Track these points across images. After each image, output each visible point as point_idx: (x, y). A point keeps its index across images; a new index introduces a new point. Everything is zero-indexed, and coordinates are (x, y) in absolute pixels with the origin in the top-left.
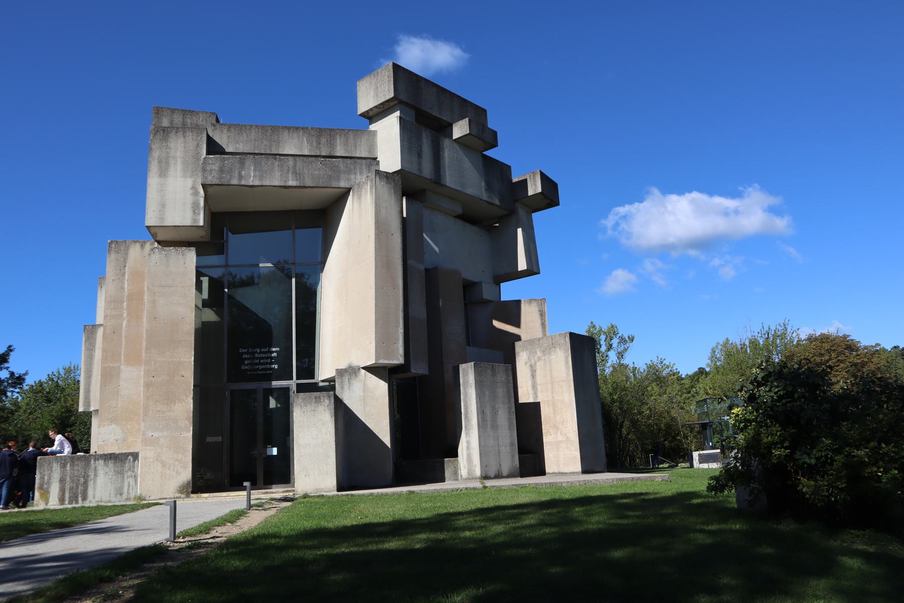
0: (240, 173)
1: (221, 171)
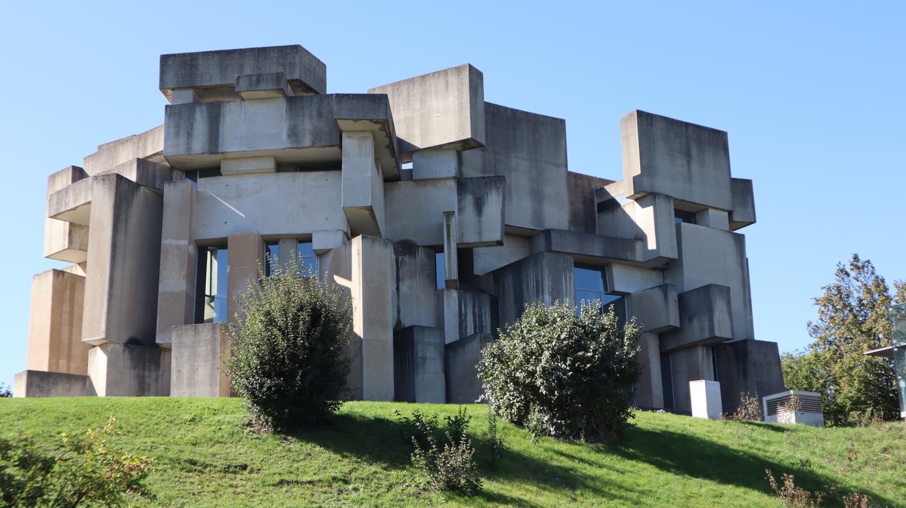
0: (65, 201)
1: (57, 203)
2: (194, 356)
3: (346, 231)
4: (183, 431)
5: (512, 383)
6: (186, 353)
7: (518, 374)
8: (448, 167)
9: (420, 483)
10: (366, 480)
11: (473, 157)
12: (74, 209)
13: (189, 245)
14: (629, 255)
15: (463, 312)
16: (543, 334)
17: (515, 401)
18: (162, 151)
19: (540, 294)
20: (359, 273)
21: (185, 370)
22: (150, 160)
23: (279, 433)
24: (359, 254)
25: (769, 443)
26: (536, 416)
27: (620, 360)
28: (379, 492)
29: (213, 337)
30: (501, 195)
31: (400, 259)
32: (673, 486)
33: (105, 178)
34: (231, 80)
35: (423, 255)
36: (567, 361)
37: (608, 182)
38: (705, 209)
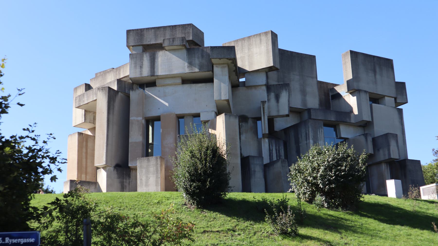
1: (79, 101)
2: (148, 172)
3: (216, 111)
4: (155, 208)
5: (306, 183)
6: (144, 171)
7: (309, 178)
8: (262, 80)
9: (269, 231)
10: (243, 230)
11: (272, 74)
12: (87, 104)
13: (143, 119)
14: (348, 120)
15: (271, 149)
16: (320, 158)
17: (307, 191)
18: (129, 75)
19: (308, 140)
20: (224, 131)
21: (144, 178)
22: (122, 79)
23: (200, 208)
24: (223, 122)
25: (428, 209)
26: (319, 198)
27: (358, 171)
28: (250, 235)
29: (156, 163)
30: (288, 93)
31: (241, 124)
32: (387, 231)
33: (102, 89)
34: (159, 41)
35: (251, 122)
36: (332, 172)
37: (336, 85)
38: (384, 97)
